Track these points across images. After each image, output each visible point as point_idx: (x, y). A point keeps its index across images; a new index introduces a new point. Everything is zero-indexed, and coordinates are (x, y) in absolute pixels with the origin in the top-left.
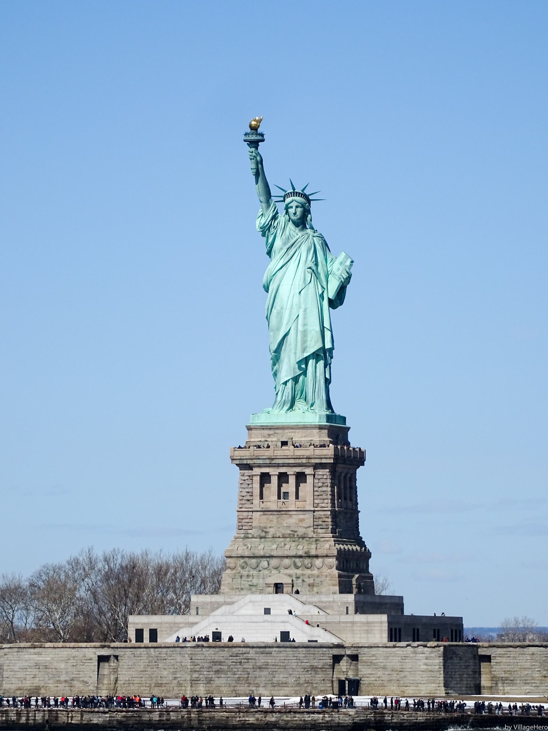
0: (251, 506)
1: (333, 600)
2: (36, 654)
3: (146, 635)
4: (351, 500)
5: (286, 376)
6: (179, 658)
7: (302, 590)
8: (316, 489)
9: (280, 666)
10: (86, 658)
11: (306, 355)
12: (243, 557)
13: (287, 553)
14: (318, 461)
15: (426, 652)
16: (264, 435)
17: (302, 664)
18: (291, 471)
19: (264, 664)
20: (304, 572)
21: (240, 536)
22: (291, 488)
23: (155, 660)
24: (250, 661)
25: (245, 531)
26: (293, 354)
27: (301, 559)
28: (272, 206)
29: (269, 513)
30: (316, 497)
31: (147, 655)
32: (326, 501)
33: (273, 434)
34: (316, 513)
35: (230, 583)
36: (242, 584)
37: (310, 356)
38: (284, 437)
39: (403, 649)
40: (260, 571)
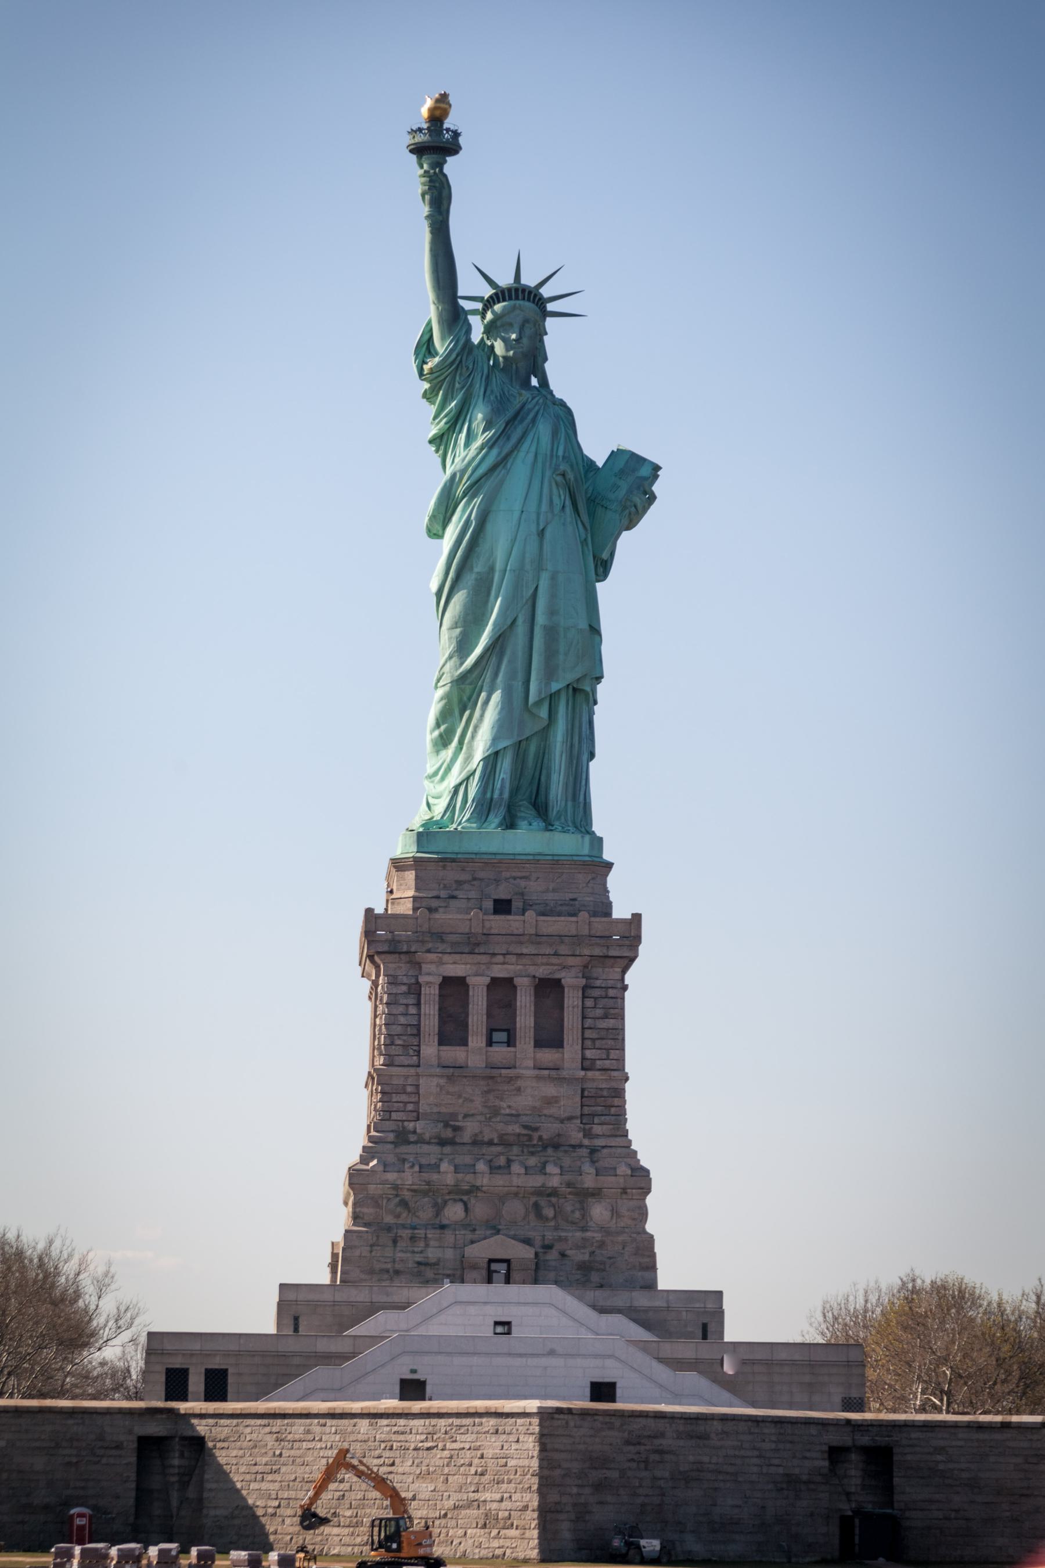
1: (665, 1305)
3: (196, 1382)
6: (492, 1446)
7: (562, 1278)
8: (588, 1023)
11: (555, 687)
14: (597, 951)
16: (445, 882)
17: (773, 1470)
22: (523, 1017)
24: (667, 1457)
26: (520, 683)
27: (554, 1200)
28: (462, 317)
30: (588, 1043)
31: (338, 1437)
32: (613, 1054)
33: (470, 881)
35: (365, 1257)
36: (397, 1259)
37: (559, 691)
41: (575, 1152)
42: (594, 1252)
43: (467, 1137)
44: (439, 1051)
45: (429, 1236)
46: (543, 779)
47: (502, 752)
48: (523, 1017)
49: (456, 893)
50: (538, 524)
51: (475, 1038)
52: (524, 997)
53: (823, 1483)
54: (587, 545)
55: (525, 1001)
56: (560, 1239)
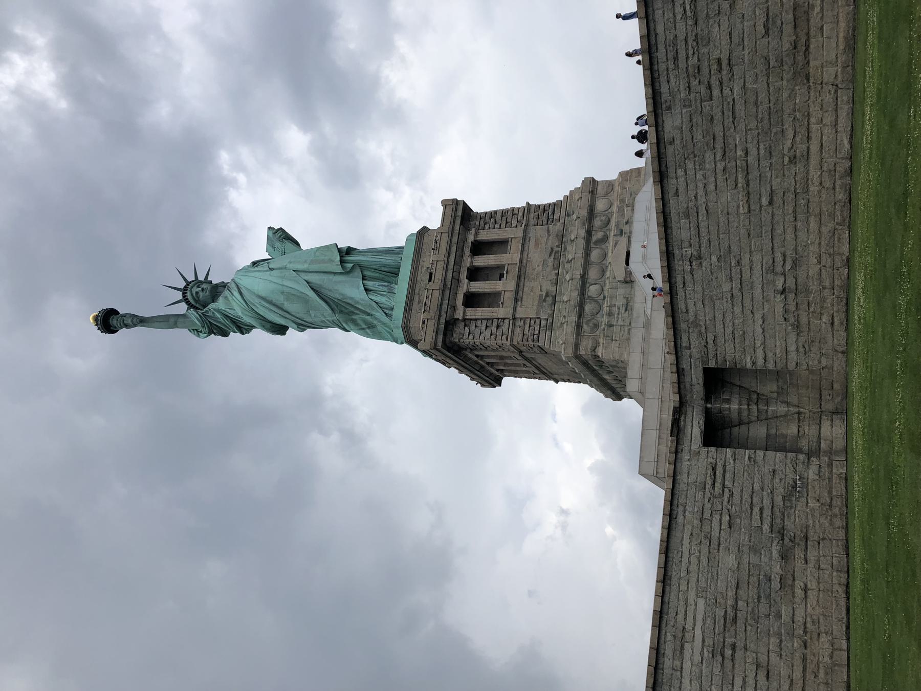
0: (507, 321)
2: (682, 647)
10: (709, 481)
11: (338, 259)
12: (579, 326)
13: (580, 254)
16: (418, 309)
18: (467, 262)
21: (548, 335)
23: (703, 89)
29: (520, 292)
31: (690, 165)
33: (419, 297)
34: (531, 223)
36: (622, 323)
38: (423, 278)
41: (567, 225)
46: (386, 269)
47: (365, 286)
49: (424, 303)
50: (267, 271)
51: (497, 287)
55: (481, 261)
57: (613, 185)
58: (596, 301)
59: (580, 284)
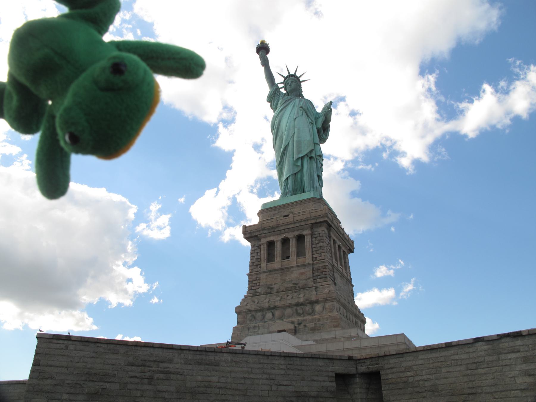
1: (334, 336)
4: (346, 270)
5: (286, 175)
8: (314, 246)
9: (236, 390)
11: (301, 155)
12: (250, 311)
13: (289, 302)
14: (313, 221)
15: (521, 349)
17: (282, 388)
19: (202, 385)
20: (305, 318)
22: (292, 248)
24: (172, 376)
25: (254, 291)
27: (302, 307)
29: (274, 272)
30: (314, 252)
32: (323, 254)
39: (467, 350)
40: (265, 322)
41: (310, 289)
42: (316, 323)
43: (275, 291)
44: (266, 265)
45: (259, 325)
47: (288, 179)
48: (292, 248)
51: (277, 258)
52: (292, 242)
53: (331, 397)
54: (314, 125)
55: (293, 243)
56: (304, 320)
57: (332, 311)
58: (264, 317)
59: (272, 306)
